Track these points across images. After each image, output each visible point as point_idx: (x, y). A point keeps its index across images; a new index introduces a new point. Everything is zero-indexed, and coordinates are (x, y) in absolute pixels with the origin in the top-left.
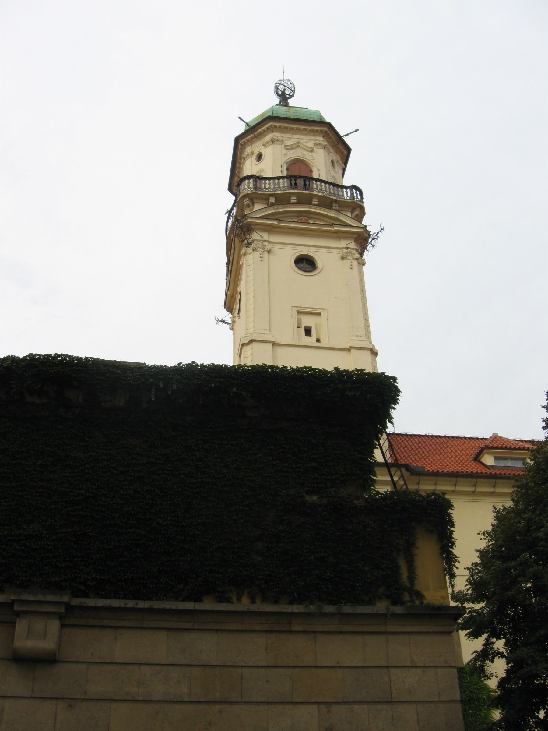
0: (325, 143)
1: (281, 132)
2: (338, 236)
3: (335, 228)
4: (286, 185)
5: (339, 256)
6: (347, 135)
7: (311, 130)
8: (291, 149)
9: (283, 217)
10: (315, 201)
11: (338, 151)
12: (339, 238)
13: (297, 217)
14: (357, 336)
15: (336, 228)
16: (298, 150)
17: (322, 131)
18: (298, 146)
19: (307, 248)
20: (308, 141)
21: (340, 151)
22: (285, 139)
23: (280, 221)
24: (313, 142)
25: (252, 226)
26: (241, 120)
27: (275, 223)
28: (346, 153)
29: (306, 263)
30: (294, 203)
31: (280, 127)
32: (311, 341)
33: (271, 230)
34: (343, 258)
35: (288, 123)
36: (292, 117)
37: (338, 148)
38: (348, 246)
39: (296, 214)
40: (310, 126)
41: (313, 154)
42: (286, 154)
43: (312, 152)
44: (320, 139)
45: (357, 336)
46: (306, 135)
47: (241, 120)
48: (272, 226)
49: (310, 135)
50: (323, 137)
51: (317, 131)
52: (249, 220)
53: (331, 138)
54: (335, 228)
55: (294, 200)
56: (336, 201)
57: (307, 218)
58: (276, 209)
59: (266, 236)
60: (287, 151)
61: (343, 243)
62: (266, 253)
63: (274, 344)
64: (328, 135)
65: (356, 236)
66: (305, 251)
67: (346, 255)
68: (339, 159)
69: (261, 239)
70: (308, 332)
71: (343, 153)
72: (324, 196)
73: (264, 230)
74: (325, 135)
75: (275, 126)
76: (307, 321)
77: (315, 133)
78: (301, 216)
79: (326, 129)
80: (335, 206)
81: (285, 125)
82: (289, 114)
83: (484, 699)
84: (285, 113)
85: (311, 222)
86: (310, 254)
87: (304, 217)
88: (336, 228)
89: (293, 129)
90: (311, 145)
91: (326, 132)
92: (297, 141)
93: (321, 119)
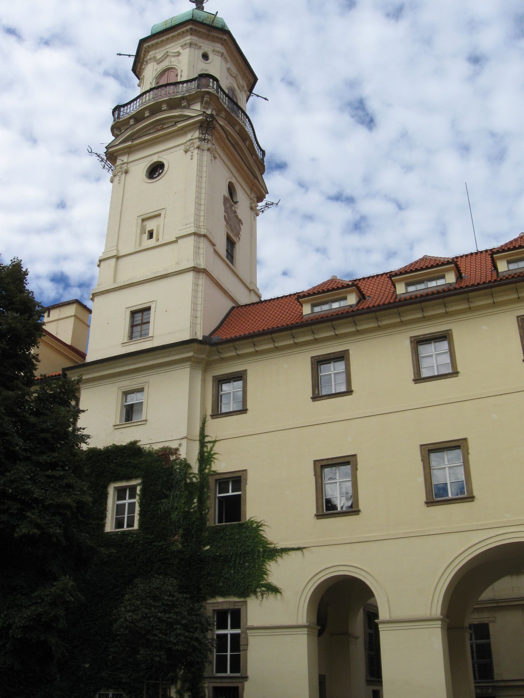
0: (195, 39)
1: (156, 49)
2: (183, 131)
3: (178, 126)
5: (182, 151)
7: (178, 35)
8: (162, 62)
10: (164, 107)
11: (214, 39)
12: (186, 133)
13: (154, 128)
14: (187, 224)
15: (180, 125)
16: (168, 59)
17: (187, 31)
18: (168, 56)
19: (157, 155)
20: (174, 47)
21: (218, 38)
25: (115, 154)
26: (120, 55)
27: (129, 143)
28: (225, 37)
29: (155, 170)
30: (148, 117)
31: (152, 45)
32: (152, 242)
34: (186, 152)
35: (158, 38)
38: (193, 138)
39: (151, 127)
40: (177, 30)
41: (180, 58)
42: (156, 69)
43: (178, 56)
44: (188, 39)
45: (187, 224)
46: (176, 41)
47: (120, 55)
48: (129, 147)
49: (180, 39)
50: (191, 35)
51: (183, 32)
53: (199, 32)
54: (178, 126)
55: (147, 114)
56: (183, 98)
57: (161, 126)
58: (133, 129)
59: (125, 159)
60: (158, 66)
61: (189, 137)
62: (124, 175)
63: (118, 258)
64: (195, 30)
65: (199, 125)
66: (155, 159)
68: (219, 47)
69: (122, 162)
70: (151, 235)
71: (221, 39)
72: (170, 99)
73: (123, 154)
74: (192, 32)
75: (149, 46)
76: (150, 225)
77: (183, 34)
78: (155, 126)
79: (190, 26)
80: (184, 103)
81: (156, 41)
83: (259, 551)
86: (160, 160)
88: (180, 125)
89: (162, 41)
91: (191, 29)
92: (165, 52)
93: (193, 16)
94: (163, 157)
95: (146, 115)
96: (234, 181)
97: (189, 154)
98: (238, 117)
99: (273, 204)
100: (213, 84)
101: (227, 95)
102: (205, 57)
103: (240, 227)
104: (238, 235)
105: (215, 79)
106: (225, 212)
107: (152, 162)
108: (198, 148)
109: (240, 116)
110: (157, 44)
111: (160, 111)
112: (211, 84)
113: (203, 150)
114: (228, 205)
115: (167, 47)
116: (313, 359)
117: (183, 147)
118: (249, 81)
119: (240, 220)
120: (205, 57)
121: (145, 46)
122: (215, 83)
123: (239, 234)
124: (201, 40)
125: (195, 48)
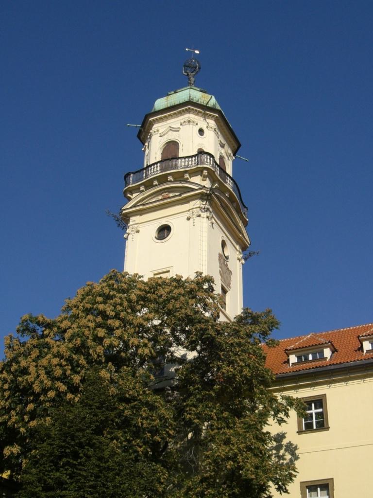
2: (187, 200)
4: (159, 168)
6: (207, 104)
9: (146, 201)
10: (170, 178)
12: (188, 202)
20: (175, 122)
22: (159, 128)
23: (144, 205)
24: (180, 122)
29: (164, 231)
31: (157, 119)
33: (141, 213)
34: (188, 219)
35: (162, 114)
36: (169, 106)
37: (207, 114)
40: (177, 109)
44: (187, 116)
52: (124, 212)
53: (196, 111)
65: (200, 196)
66: (164, 222)
67: (191, 216)
75: (153, 120)
78: (162, 193)
82: (166, 103)
84: (164, 104)
85: (171, 195)
87: (165, 193)
89: (165, 117)
90: (178, 126)
92: (168, 126)
93: (190, 96)
94: (170, 221)
95: (154, 184)
96: (225, 239)
97: (191, 220)
98: (226, 182)
99: (254, 253)
100: (207, 159)
101: (218, 166)
102: (201, 132)
103: (230, 277)
104: (229, 285)
105: (211, 156)
106: (220, 267)
107: (160, 225)
108: (199, 216)
109: (228, 182)
110: (161, 118)
111: (167, 181)
112: (209, 161)
113: (203, 217)
114: (222, 260)
115: (169, 121)
116: (309, 415)
117: (188, 214)
118: (234, 147)
119: (231, 272)
120: (201, 132)
121: (150, 119)
122: (211, 159)
123: (230, 283)
124: (196, 117)
125: (193, 125)
